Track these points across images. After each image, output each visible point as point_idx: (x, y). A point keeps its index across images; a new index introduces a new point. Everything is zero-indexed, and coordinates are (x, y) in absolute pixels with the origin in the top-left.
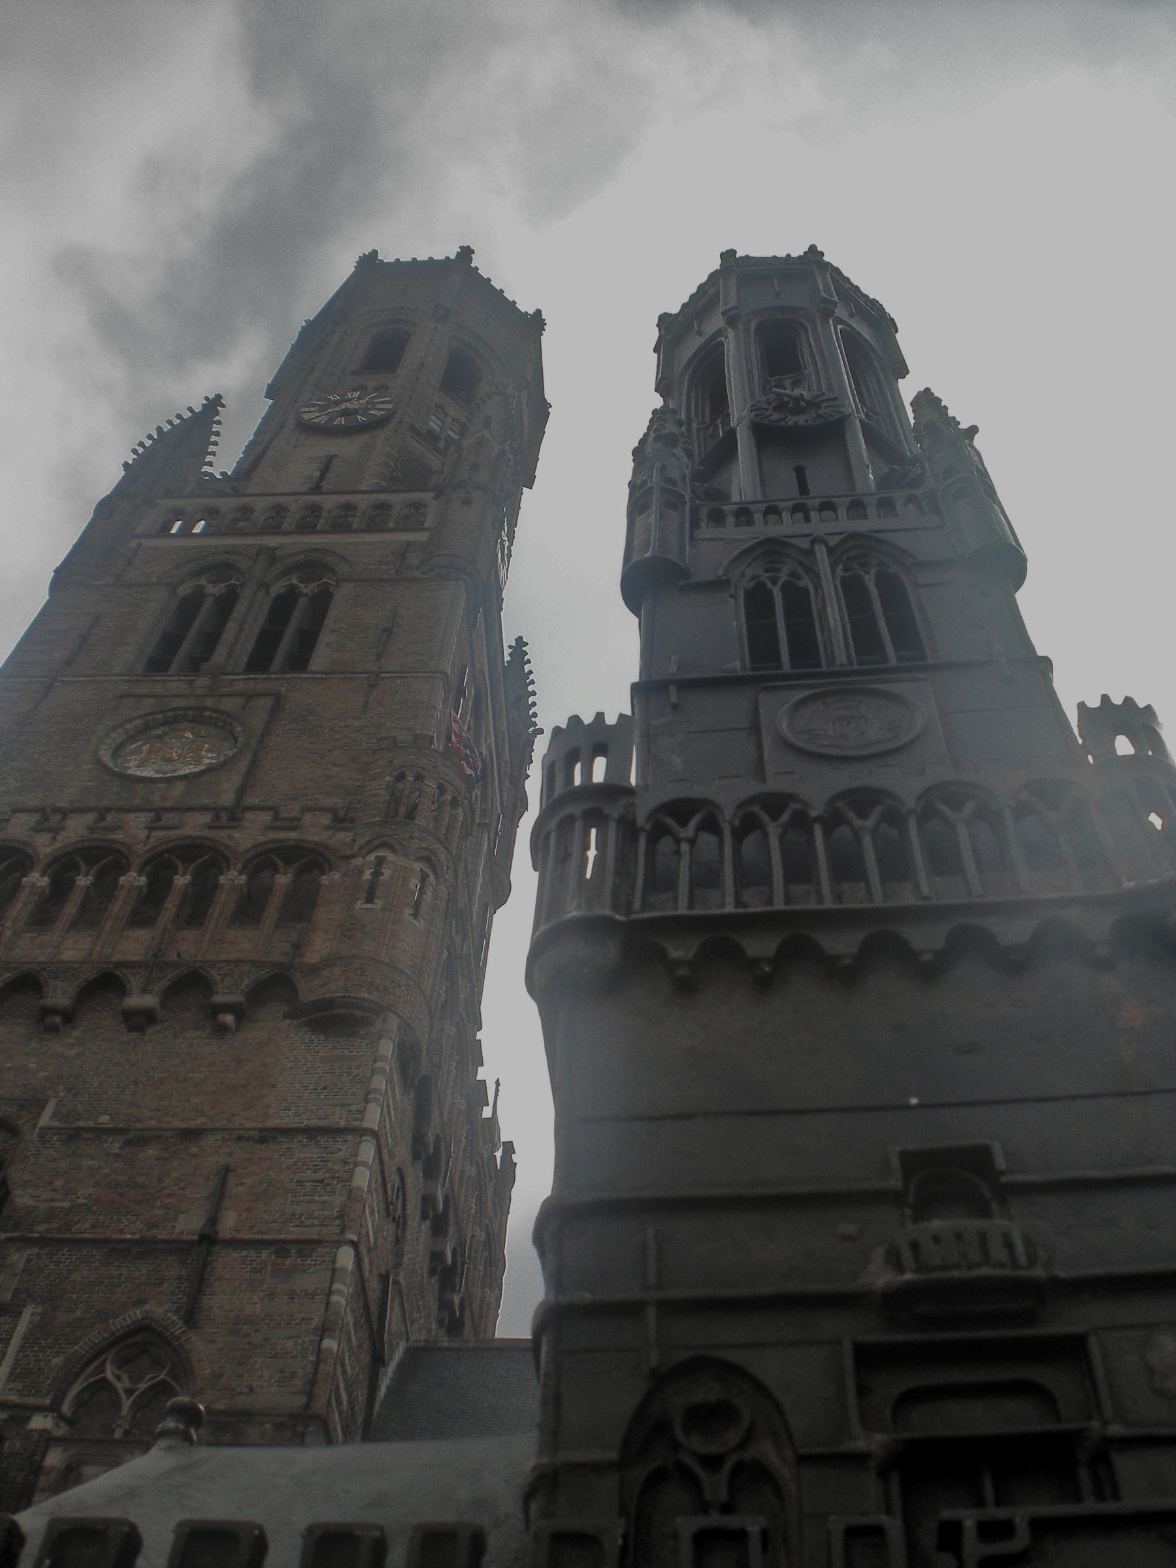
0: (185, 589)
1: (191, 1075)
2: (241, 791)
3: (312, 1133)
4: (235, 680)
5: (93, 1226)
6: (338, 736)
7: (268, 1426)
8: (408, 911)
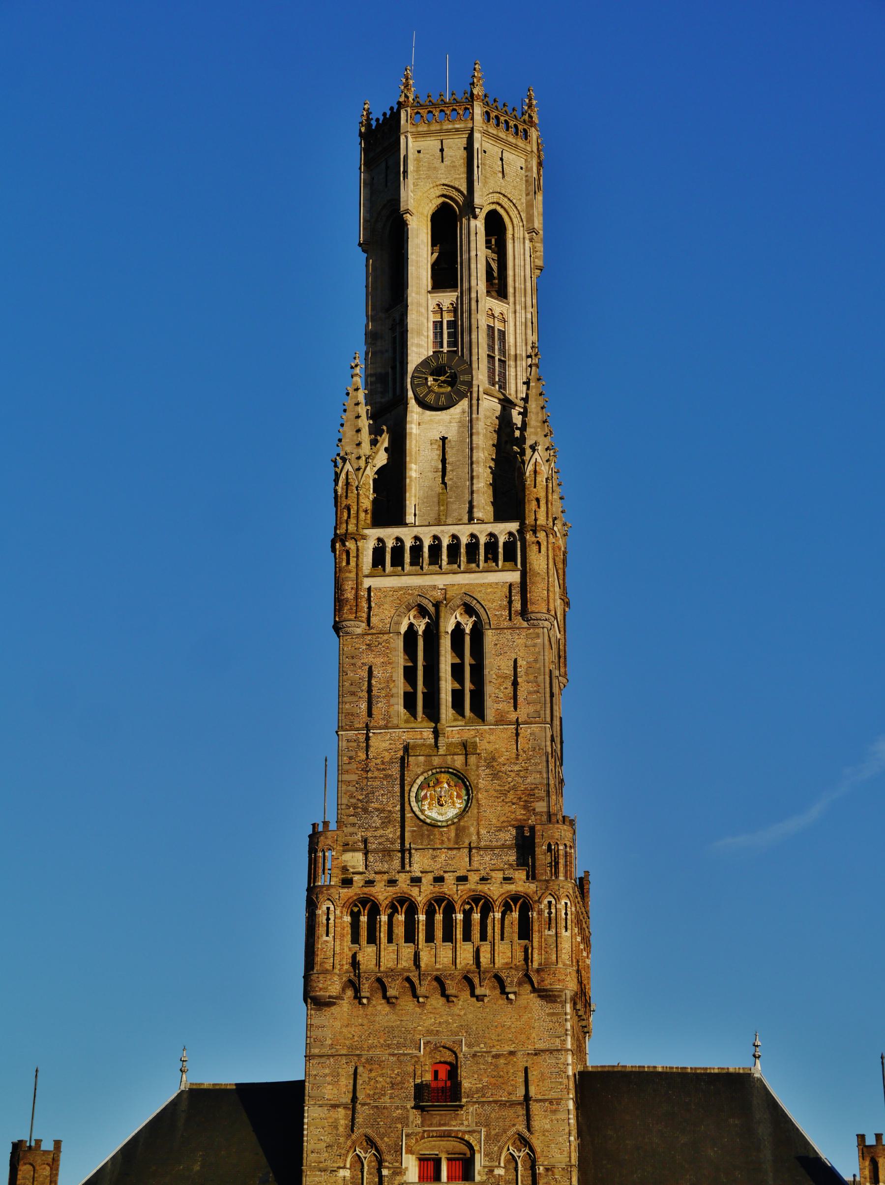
0: (403, 628)
1: (506, 1023)
2: (478, 833)
3: (551, 1051)
4: (452, 731)
5: (492, 1095)
6: (510, 779)
7: (560, 1169)
8: (564, 930)
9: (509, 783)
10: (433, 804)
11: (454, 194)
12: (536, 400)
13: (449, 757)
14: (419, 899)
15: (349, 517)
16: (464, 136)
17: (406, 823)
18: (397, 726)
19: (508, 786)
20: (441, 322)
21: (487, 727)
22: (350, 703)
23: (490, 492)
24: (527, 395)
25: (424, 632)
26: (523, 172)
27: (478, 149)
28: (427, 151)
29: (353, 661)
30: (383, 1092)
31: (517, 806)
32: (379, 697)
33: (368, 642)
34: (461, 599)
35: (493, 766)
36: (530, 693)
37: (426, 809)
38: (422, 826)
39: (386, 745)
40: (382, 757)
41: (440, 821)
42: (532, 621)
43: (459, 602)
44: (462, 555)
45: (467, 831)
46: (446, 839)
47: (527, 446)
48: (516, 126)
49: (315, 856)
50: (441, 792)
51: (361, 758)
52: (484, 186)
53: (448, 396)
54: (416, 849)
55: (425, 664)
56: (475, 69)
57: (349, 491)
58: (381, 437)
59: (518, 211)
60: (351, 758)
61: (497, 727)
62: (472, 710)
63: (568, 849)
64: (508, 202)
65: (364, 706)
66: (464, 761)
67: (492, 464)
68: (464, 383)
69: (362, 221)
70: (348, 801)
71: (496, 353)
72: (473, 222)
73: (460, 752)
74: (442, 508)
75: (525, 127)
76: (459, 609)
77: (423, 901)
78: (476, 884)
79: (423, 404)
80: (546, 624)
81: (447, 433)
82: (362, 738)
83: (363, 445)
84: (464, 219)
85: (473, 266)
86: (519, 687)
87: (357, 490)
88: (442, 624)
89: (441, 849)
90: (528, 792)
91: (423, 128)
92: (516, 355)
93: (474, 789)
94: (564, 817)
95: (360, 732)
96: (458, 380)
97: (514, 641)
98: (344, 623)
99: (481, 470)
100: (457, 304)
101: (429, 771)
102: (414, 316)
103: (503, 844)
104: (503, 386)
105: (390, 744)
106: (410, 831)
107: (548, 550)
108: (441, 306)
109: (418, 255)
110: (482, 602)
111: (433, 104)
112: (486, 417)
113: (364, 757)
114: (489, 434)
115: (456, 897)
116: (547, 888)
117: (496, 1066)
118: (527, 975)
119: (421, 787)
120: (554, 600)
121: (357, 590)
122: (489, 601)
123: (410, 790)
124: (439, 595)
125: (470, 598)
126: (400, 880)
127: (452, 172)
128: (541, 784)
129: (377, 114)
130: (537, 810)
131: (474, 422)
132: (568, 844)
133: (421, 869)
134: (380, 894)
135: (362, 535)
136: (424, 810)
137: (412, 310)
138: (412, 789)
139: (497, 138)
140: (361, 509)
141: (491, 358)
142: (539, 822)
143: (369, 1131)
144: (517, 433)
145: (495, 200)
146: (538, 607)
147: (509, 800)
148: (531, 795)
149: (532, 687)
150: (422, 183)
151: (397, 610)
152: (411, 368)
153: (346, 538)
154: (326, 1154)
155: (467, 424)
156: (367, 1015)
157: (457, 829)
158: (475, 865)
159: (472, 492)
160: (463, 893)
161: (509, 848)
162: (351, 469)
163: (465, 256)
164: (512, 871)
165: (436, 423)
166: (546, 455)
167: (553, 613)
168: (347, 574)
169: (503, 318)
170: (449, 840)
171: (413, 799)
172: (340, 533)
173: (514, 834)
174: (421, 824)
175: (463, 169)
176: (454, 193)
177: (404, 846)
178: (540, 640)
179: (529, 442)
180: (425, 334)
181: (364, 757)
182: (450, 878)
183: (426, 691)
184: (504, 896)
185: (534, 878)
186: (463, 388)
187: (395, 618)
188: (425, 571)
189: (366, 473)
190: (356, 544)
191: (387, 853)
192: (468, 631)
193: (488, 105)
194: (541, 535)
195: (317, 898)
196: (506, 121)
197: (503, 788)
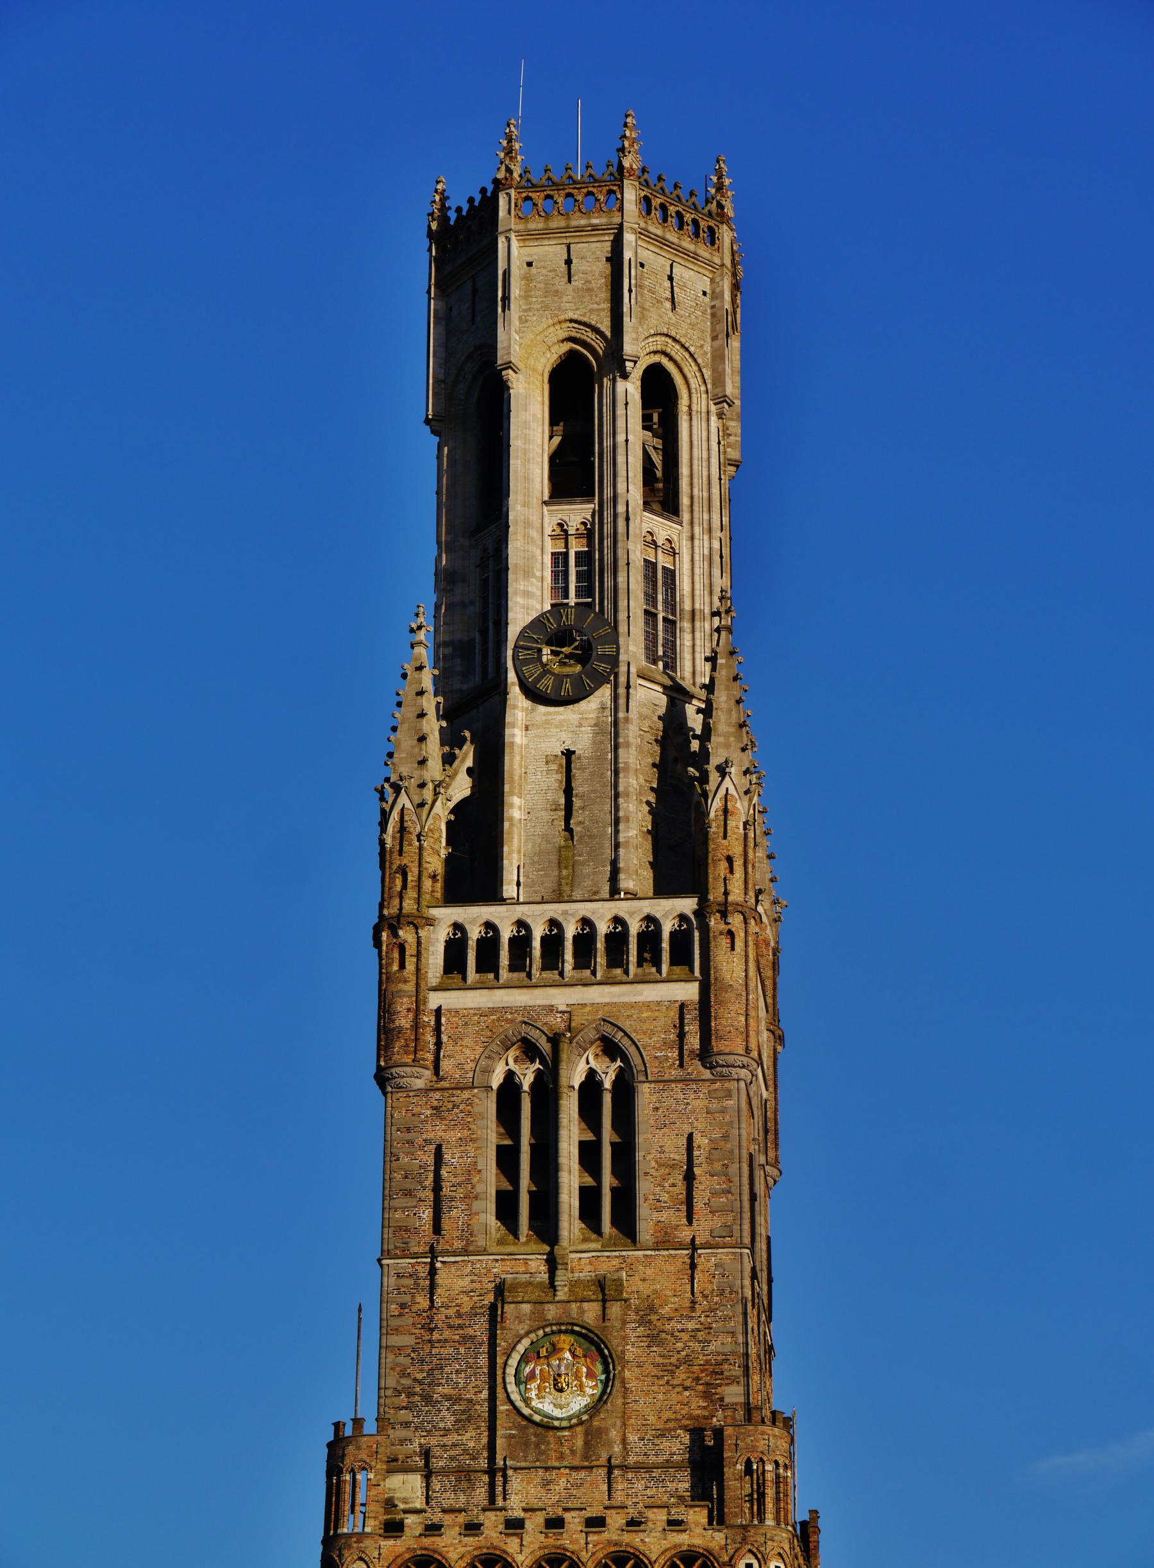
0: (497, 1080)
2: (624, 1441)
4: (580, 1258)
6: (680, 1345)
9: (678, 1352)
10: (545, 1388)
11: (590, 337)
12: (727, 688)
13: (574, 1306)
14: (519, 1558)
15: (404, 886)
16: (607, 238)
17: (498, 1422)
18: (485, 1250)
19: (676, 1356)
20: (566, 555)
21: (641, 1253)
22: (404, 1209)
23: (648, 845)
24: (712, 679)
25: (533, 1086)
26: (707, 299)
27: (630, 259)
28: (543, 263)
31: (693, 1393)
32: (452, 1199)
33: (435, 1103)
34: (598, 1030)
35: (650, 1322)
36: (714, 1194)
37: (534, 1396)
38: (526, 1427)
39: (464, 1283)
40: (457, 1305)
41: (558, 1419)
42: (718, 1069)
43: (593, 1035)
44: (599, 954)
45: (604, 1437)
46: (568, 1451)
47: (711, 767)
48: (695, 222)
49: (338, 1480)
50: (559, 1366)
51: (420, 1307)
52: (640, 323)
53: (577, 680)
54: (515, 1469)
55: (533, 1141)
56: (626, 125)
57: (405, 843)
58: (460, 749)
59: (698, 365)
60: (403, 1306)
61: (657, 1253)
62: (614, 1223)
63: (781, 1471)
64: (682, 351)
65: (427, 1214)
66: (600, 1313)
67: (652, 798)
68: (603, 658)
69: (431, 381)
70: (398, 1382)
71: (660, 607)
72: (621, 385)
73: (594, 1297)
74: (564, 872)
75: (712, 223)
76: (594, 1047)
77: (526, 1563)
78: (619, 1532)
79: (534, 695)
80: (744, 1073)
81: (574, 743)
82: (423, 1271)
83: (430, 763)
84: (605, 380)
85: (621, 459)
86: (696, 1184)
87: (419, 840)
88: (563, 1073)
89: (559, 1468)
90: (711, 1368)
91: (537, 224)
92: (693, 611)
93: (616, 1363)
94: (774, 1413)
95: (419, 1260)
96: (594, 654)
97: (688, 1104)
98: (393, 1070)
99: (632, 807)
100: (593, 524)
101: (538, 1329)
102: (519, 544)
103: (667, 1461)
104: (671, 665)
105: (472, 1281)
106: (503, 1436)
107: (746, 946)
108: (565, 527)
109: (526, 439)
110: (633, 1035)
111: (554, 184)
112: (642, 717)
113: (423, 1302)
114: (647, 747)
115: (584, 1556)
116: (744, 1539)
119: (524, 1359)
120: (758, 1033)
121: (417, 1012)
122: (645, 1034)
123: (505, 1364)
124: (558, 1022)
125: (613, 1027)
126: (487, 1523)
127: (585, 300)
128: (733, 1353)
129: (459, 200)
130: (727, 1400)
131: (621, 725)
132: (781, 1461)
133: (523, 1505)
134: (451, 1549)
135: (427, 919)
136: (531, 1399)
137: (515, 534)
138: (510, 1362)
139: (663, 242)
140: (425, 874)
141: (650, 615)
142: (729, 1421)
144: (695, 745)
145: (659, 348)
146: (729, 1045)
147: (679, 1383)
148: (717, 1373)
149: (719, 1184)
150: (535, 318)
151: (486, 1047)
152: (513, 631)
153: (399, 922)
155: (609, 728)
157: (587, 1434)
158: (619, 1497)
159: (617, 846)
160: (598, 1548)
161: (678, 1467)
162: (408, 805)
163: (608, 443)
164: (682, 1508)
165: (556, 727)
166: (744, 783)
167: (755, 1054)
168: (401, 986)
169: (672, 548)
170: (573, 1452)
171: (510, 1379)
172: (389, 914)
173: (687, 1442)
174: (524, 1423)
175: (605, 294)
176: (590, 334)
177: (495, 1464)
178: (732, 1102)
179: (715, 761)
180: (538, 574)
181: (426, 1304)
182: (574, 1521)
183: (534, 1189)
184: (668, 1555)
185: (721, 1522)
186: (602, 667)
187: (483, 1062)
188: (534, 981)
189: (434, 811)
190: (417, 933)
191: (464, 1475)
192: (608, 1085)
193: (648, 186)
194: (736, 921)
195: (340, 1556)
196: (678, 213)
197: (668, 1361)
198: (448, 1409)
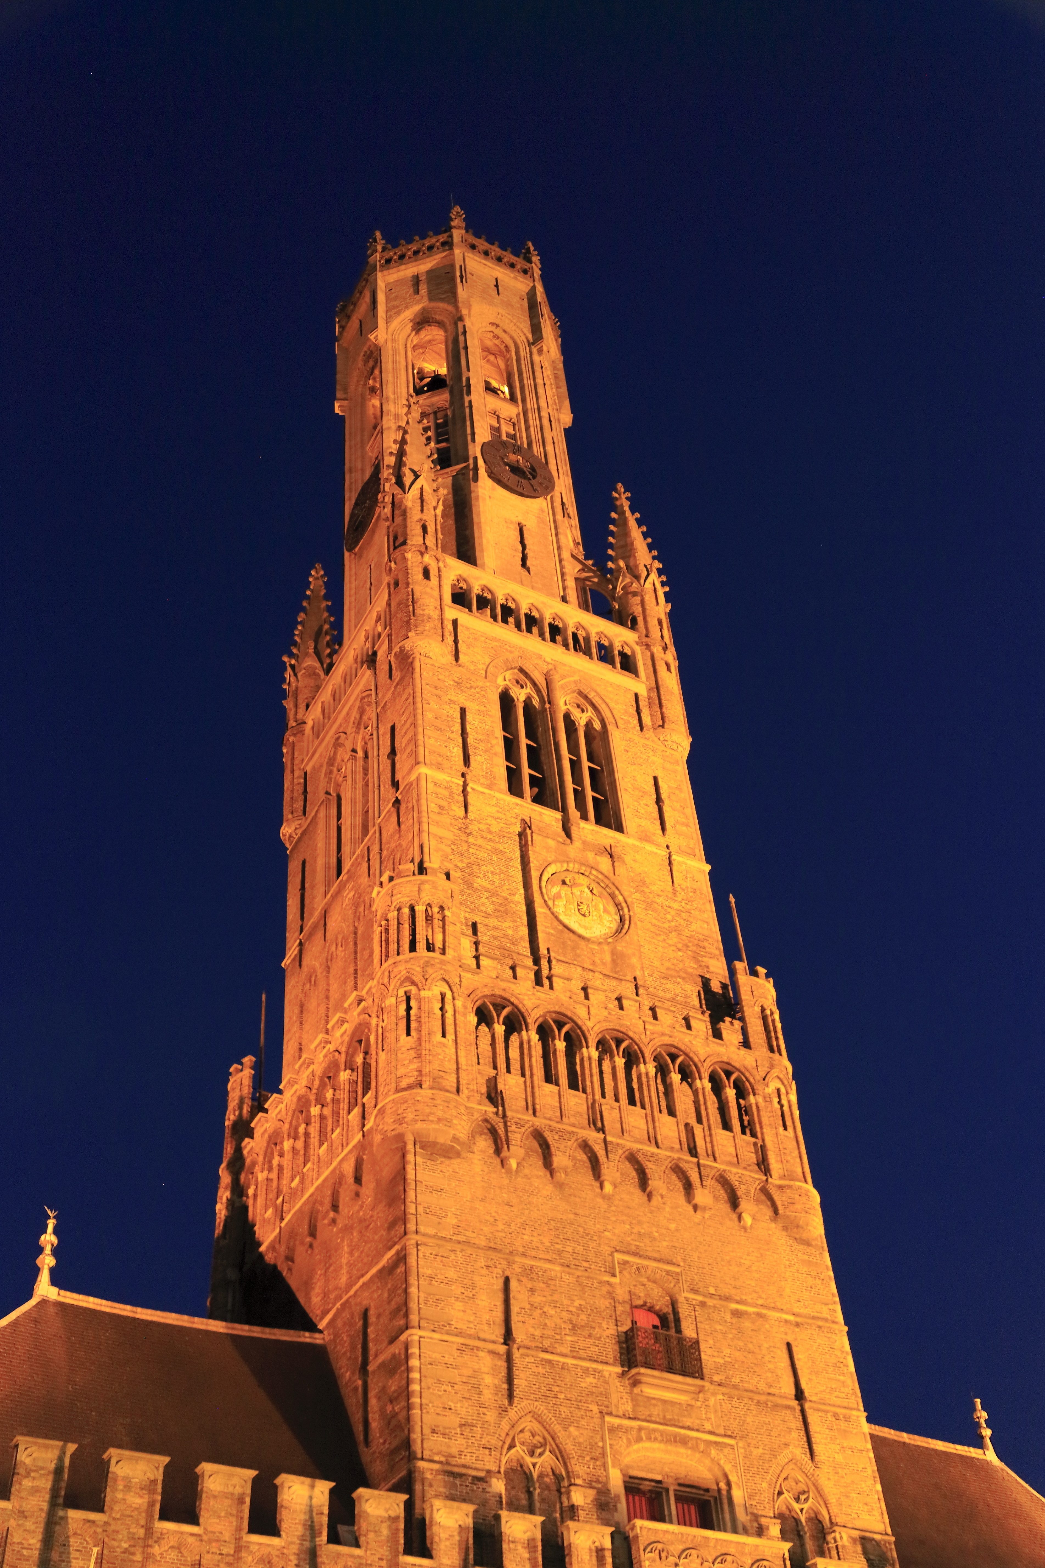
14: (590, 1024)
29: (438, 692)
30: (558, 1337)
32: (476, 748)
35: (643, 891)
37: (561, 911)
38: (562, 931)
46: (599, 962)
95: (453, 780)
105: (498, 812)
117: (740, 1331)
118: (764, 1191)
143: (541, 1407)
154: (461, 1441)
156: (516, 1190)
174: (561, 927)
187: (491, 669)
198: (487, 898)
